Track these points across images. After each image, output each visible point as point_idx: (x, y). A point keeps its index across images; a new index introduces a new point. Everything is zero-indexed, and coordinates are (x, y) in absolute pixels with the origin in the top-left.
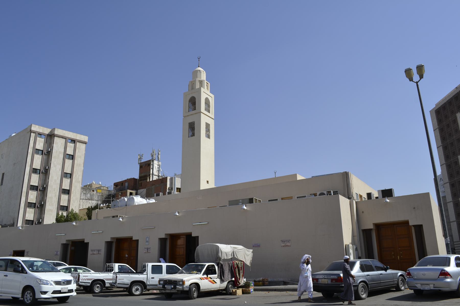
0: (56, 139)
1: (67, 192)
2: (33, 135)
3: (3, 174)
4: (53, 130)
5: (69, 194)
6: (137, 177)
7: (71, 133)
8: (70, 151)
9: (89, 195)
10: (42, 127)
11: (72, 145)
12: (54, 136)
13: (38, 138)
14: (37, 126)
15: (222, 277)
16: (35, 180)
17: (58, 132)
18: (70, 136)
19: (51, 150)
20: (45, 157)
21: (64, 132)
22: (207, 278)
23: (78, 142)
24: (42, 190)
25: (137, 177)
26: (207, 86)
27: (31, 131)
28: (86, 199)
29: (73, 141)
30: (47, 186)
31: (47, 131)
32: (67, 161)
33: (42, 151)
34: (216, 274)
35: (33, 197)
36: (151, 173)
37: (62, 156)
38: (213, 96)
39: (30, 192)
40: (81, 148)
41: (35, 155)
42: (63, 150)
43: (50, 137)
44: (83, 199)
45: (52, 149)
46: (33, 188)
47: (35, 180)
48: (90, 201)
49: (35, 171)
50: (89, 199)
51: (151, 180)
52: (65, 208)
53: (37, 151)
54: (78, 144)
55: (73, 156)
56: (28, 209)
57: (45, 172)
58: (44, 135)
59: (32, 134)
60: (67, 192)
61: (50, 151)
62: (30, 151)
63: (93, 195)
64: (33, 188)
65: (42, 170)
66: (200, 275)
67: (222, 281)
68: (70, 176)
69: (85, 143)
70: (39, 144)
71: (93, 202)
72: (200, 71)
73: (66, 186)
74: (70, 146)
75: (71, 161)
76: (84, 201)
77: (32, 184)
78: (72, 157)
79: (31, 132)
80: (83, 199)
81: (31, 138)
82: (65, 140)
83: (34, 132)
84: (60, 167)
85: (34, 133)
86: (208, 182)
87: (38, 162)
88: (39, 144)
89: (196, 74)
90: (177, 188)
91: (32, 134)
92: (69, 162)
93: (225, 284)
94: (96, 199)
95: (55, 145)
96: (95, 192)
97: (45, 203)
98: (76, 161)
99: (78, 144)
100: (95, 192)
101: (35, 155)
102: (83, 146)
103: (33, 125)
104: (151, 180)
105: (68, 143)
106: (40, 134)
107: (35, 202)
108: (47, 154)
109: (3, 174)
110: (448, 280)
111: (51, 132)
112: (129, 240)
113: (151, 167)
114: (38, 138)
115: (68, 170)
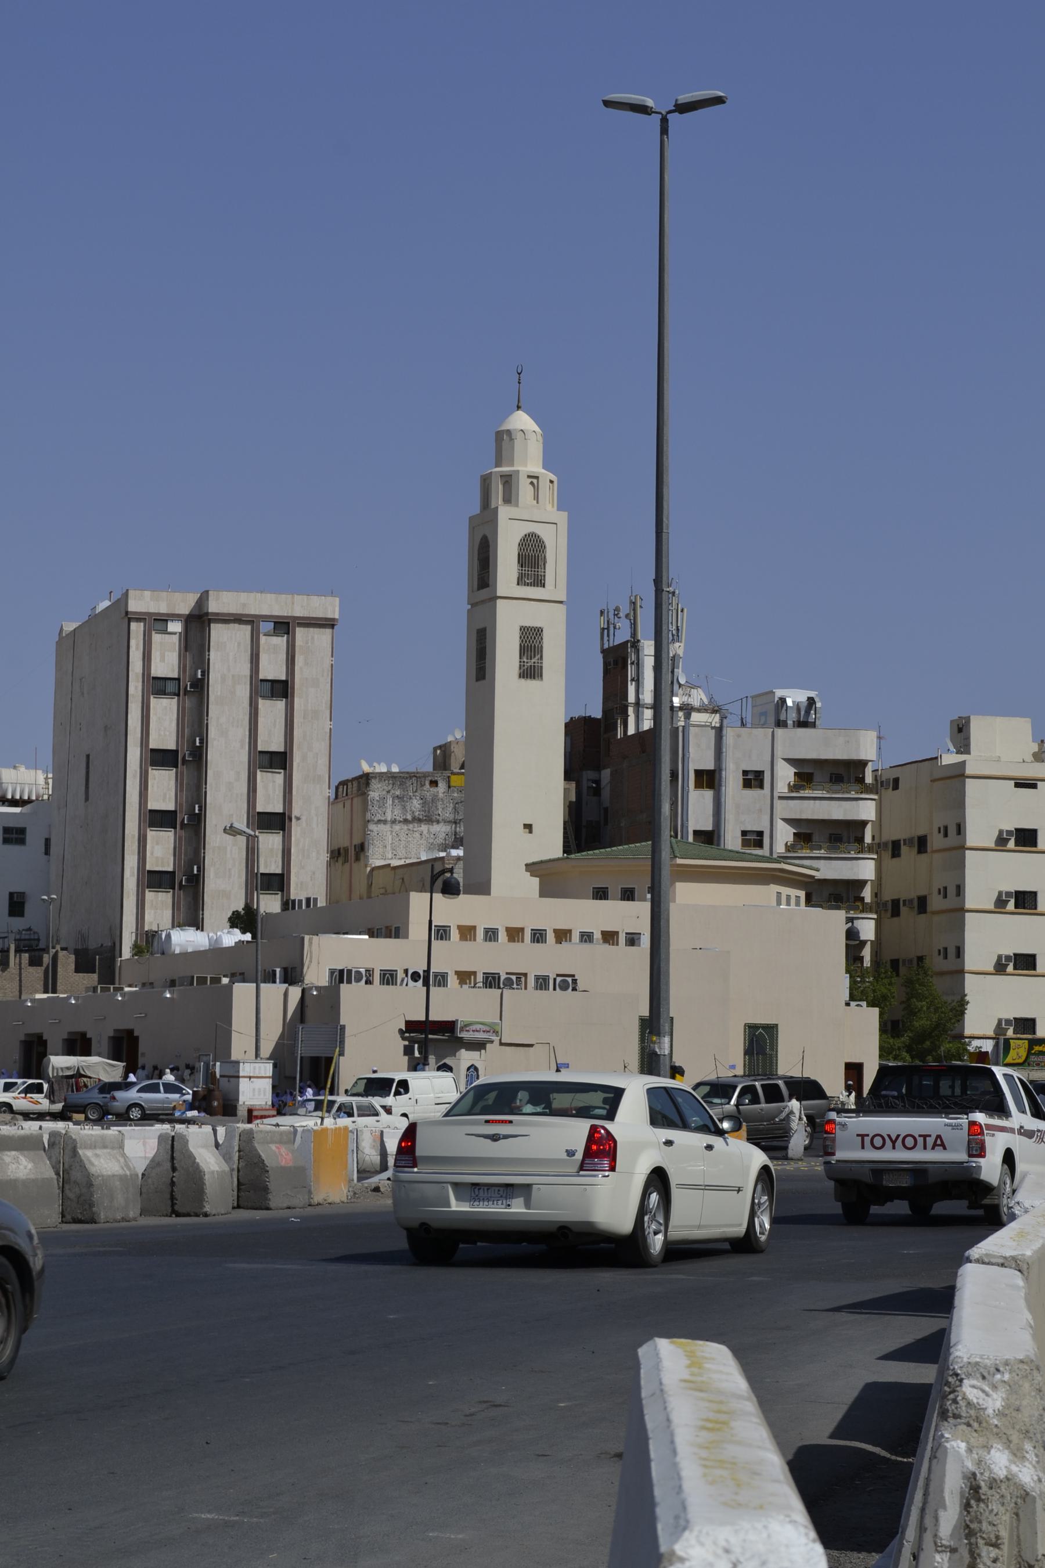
0: (218, 633)
1: (277, 822)
2: (137, 628)
3: (88, 756)
4: (203, 600)
5: (283, 828)
6: (598, 714)
7: (270, 597)
8: (272, 669)
9: (416, 804)
10: (164, 594)
11: (281, 641)
12: (210, 621)
13: (156, 638)
14: (147, 594)
15: (51, 1097)
16: (164, 790)
17: (219, 603)
18: (265, 611)
19: (203, 674)
20: (188, 703)
21: (243, 597)
22: (25, 1098)
23: (300, 625)
24: (188, 822)
25: (598, 714)
26: (536, 488)
27: (130, 618)
28: (406, 821)
29: (284, 626)
30: (203, 808)
31: (185, 604)
32: (263, 704)
33: (178, 679)
34: (42, 1092)
35: (162, 850)
36: (631, 698)
37: (244, 692)
38: (564, 515)
39: (152, 834)
40: (315, 646)
41: (154, 701)
42: (245, 669)
43: (198, 623)
44: (394, 822)
45: (206, 673)
46: (160, 819)
47: (164, 790)
48: (424, 828)
49: (161, 758)
50: (420, 821)
51: (631, 731)
52: (277, 882)
53: (158, 686)
54: (300, 633)
55: (285, 682)
56: (149, 895)
57: (189, 759)
58: (175, 617)
59: (134, 625)
60: (277, 822)
61: (202, 680)
62: (135, 688)
63: (435, 799)
64: (160, 819)
65: (185, 752)
66: (15, 1094)
67: (52, 1102)
68: (279, 761)
69: (329, 624)
70: (163, 659)
71: (436, 828)
72: (509, 432)
73: (270, 801)
74: (273, 647)
75: (280, 705)
76: (397, 827)
77: (152, 805)
78: (282, 689)
79: (130, 620)
80: (394, 822)
81: (133, 643)
82: (249, 627)
83: (140, 618)
84: (242, 732)
85: (138, 620)
86: (529, 827)
87: (164, 723)
88: (163, 659)
89: (503, 442)
90: (699, 773)
91: (134, 625)
92: (272, 710)
93: (58, 1107)
94: (448, 814)
95: (214, 656)
96: (442, 786)
97: (201, 869)
98: (298, 702)
99: (300, 633)
100: (442, 786)
101: (154, 701)
102: (322, 638)
103: (131, 593)
104: (631, 731)
105: (263, 639)
106: (159, 622)
107: (170, 869)
108: (192, 689)
109: (88, 756)
110: (116, 1104)
111: (203, 600)
112: (130, 1032)
113: (631, 671)
114: (156, 638)
115: (272, 741)
